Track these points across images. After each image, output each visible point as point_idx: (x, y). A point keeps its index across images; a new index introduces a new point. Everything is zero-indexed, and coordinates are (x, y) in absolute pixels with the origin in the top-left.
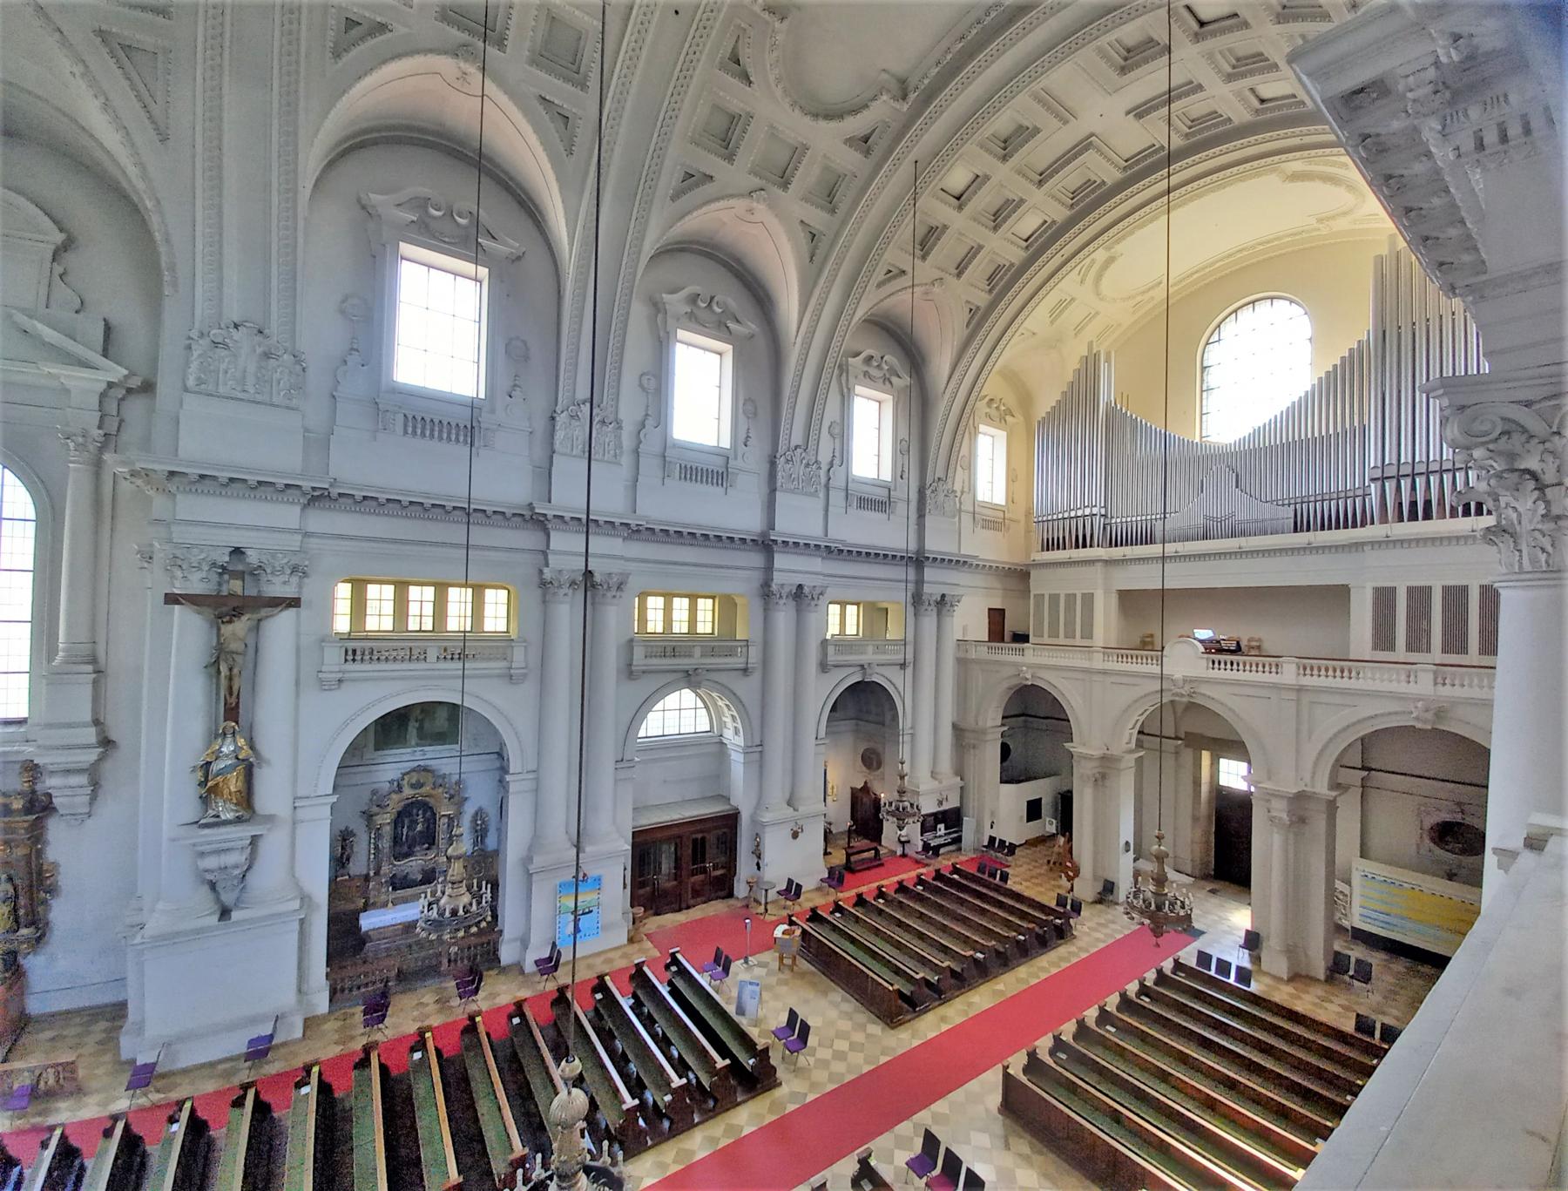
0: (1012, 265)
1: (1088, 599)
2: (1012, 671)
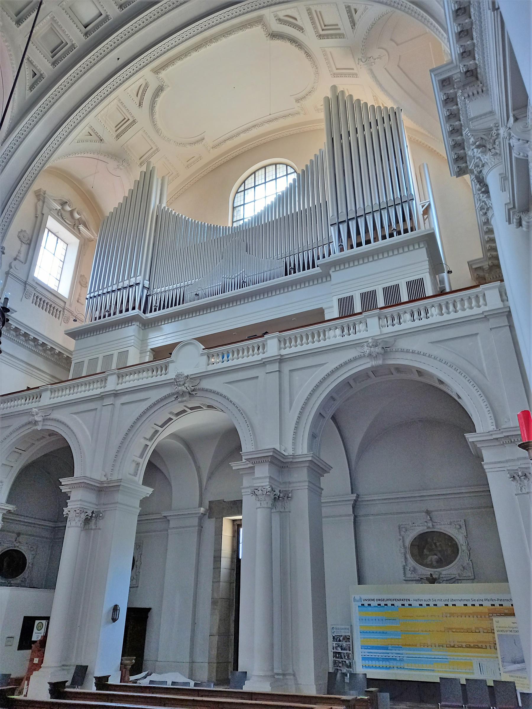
0: (73, 46)
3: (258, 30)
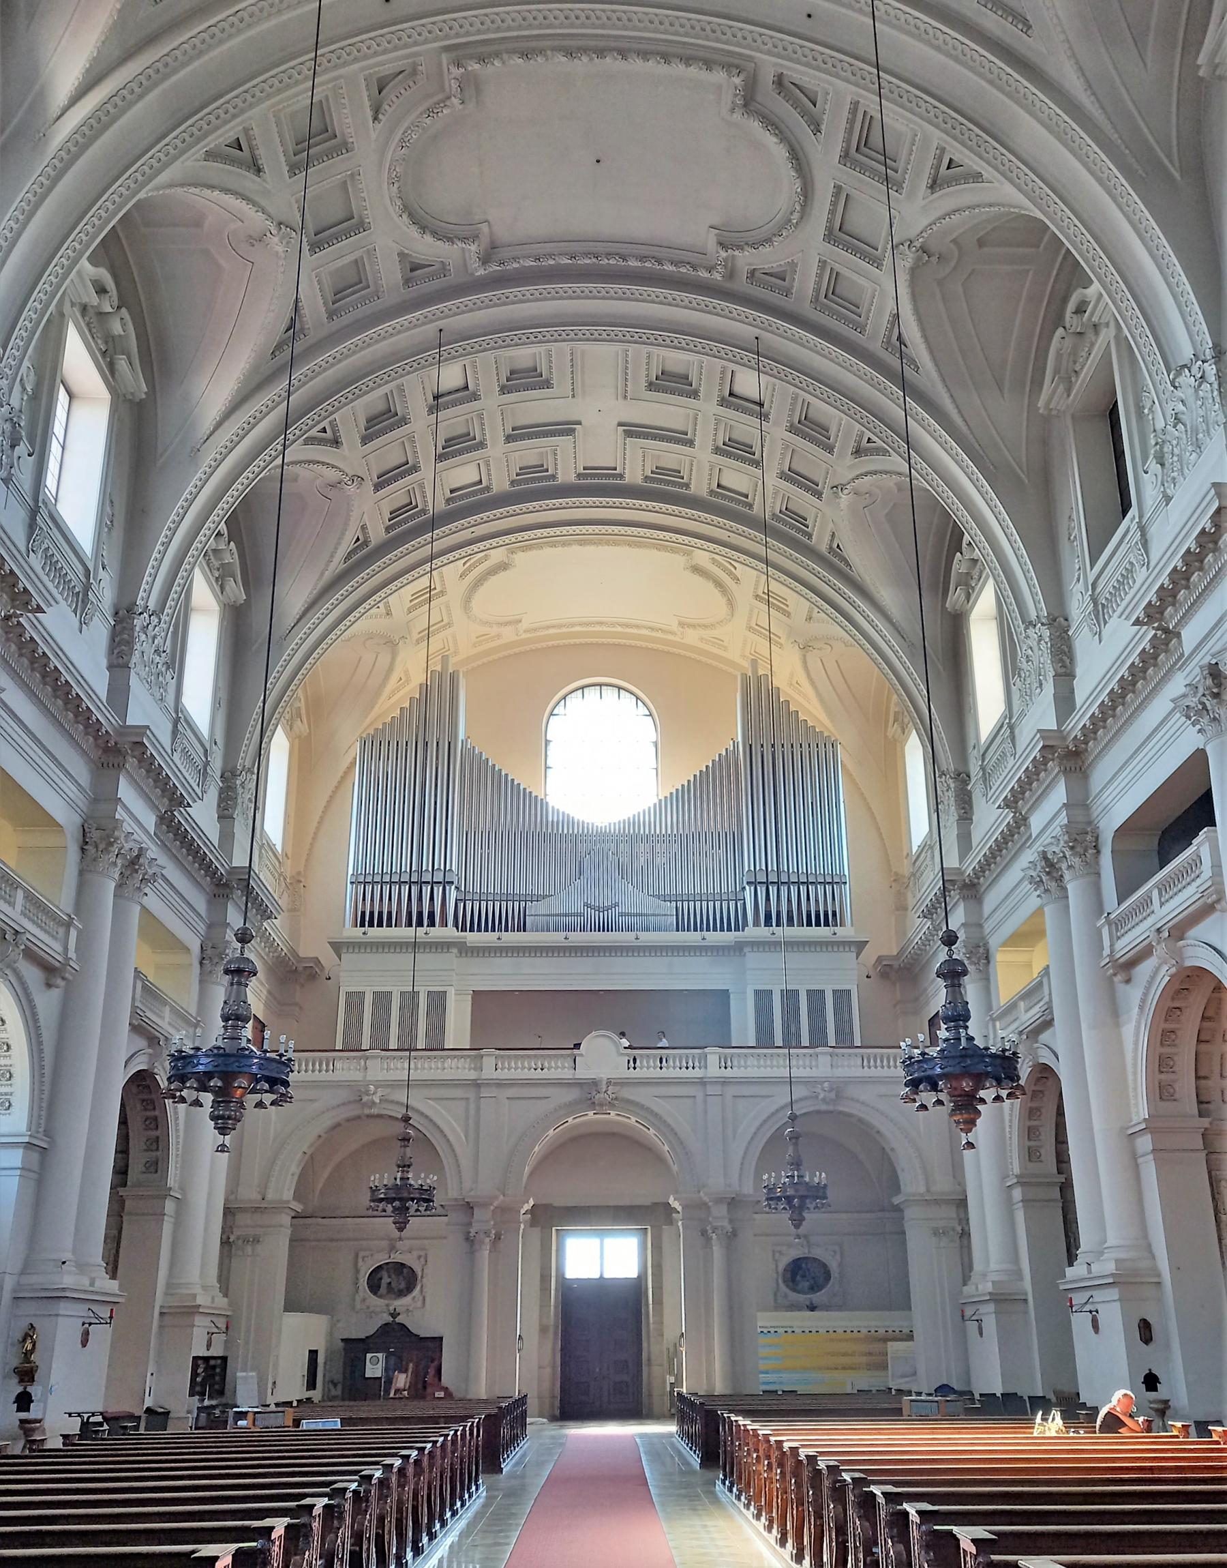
1: (438, 1001)
2: (343, 1095)
3: (680, 560)
